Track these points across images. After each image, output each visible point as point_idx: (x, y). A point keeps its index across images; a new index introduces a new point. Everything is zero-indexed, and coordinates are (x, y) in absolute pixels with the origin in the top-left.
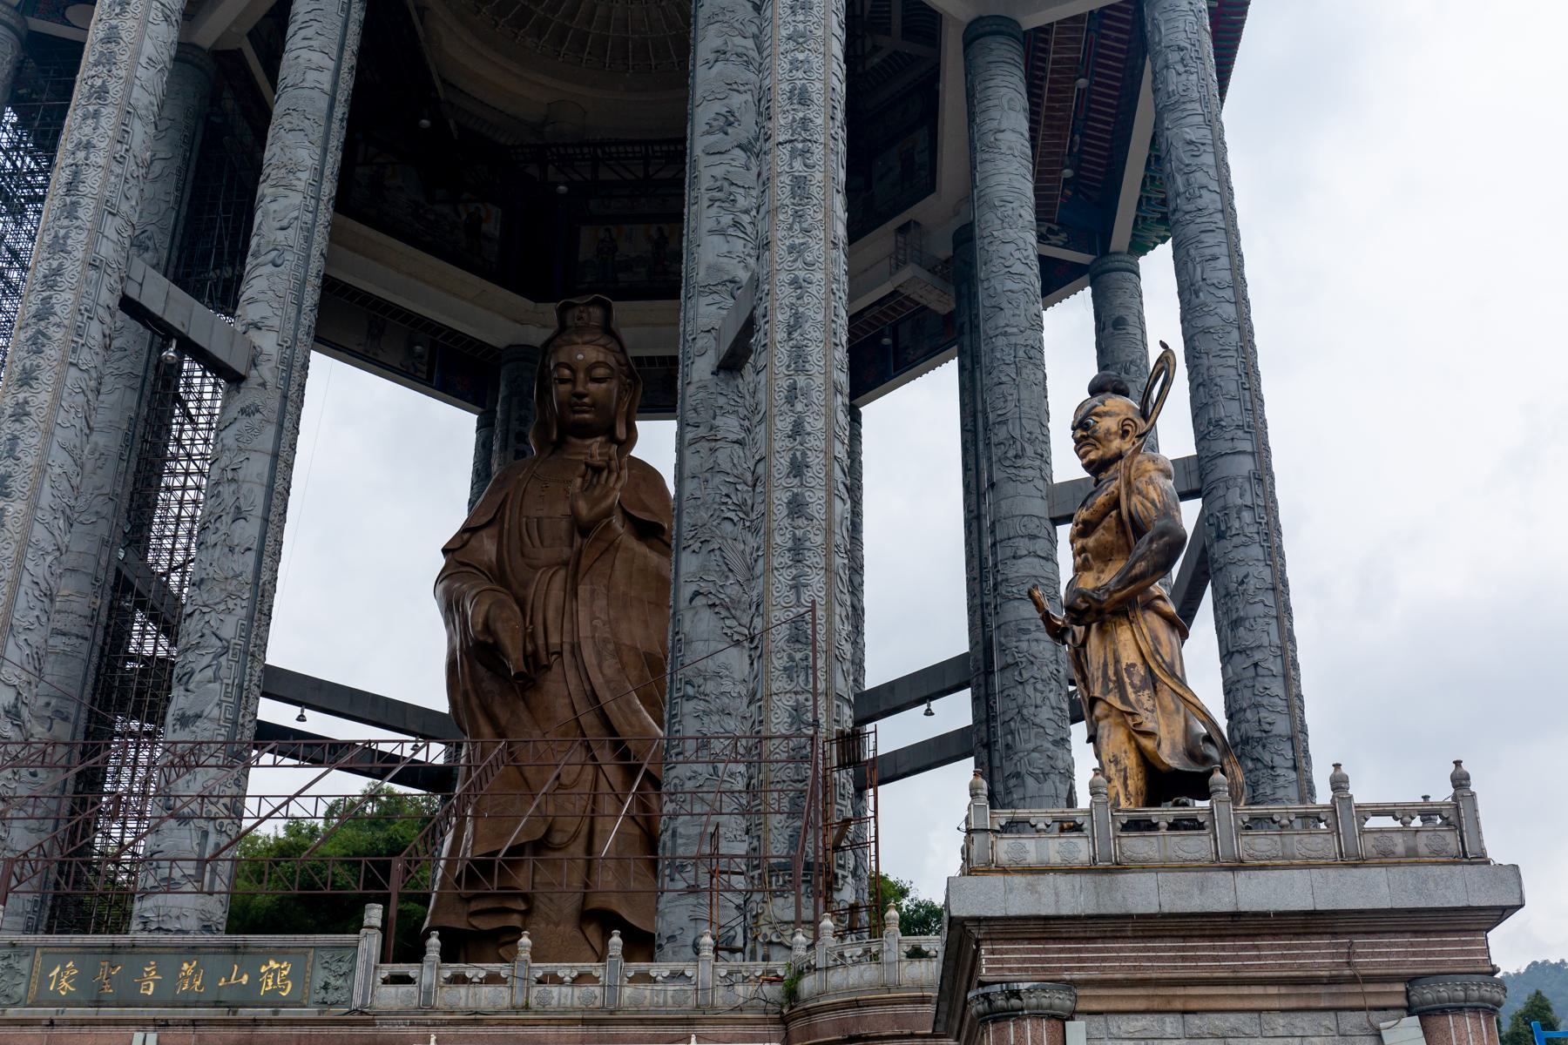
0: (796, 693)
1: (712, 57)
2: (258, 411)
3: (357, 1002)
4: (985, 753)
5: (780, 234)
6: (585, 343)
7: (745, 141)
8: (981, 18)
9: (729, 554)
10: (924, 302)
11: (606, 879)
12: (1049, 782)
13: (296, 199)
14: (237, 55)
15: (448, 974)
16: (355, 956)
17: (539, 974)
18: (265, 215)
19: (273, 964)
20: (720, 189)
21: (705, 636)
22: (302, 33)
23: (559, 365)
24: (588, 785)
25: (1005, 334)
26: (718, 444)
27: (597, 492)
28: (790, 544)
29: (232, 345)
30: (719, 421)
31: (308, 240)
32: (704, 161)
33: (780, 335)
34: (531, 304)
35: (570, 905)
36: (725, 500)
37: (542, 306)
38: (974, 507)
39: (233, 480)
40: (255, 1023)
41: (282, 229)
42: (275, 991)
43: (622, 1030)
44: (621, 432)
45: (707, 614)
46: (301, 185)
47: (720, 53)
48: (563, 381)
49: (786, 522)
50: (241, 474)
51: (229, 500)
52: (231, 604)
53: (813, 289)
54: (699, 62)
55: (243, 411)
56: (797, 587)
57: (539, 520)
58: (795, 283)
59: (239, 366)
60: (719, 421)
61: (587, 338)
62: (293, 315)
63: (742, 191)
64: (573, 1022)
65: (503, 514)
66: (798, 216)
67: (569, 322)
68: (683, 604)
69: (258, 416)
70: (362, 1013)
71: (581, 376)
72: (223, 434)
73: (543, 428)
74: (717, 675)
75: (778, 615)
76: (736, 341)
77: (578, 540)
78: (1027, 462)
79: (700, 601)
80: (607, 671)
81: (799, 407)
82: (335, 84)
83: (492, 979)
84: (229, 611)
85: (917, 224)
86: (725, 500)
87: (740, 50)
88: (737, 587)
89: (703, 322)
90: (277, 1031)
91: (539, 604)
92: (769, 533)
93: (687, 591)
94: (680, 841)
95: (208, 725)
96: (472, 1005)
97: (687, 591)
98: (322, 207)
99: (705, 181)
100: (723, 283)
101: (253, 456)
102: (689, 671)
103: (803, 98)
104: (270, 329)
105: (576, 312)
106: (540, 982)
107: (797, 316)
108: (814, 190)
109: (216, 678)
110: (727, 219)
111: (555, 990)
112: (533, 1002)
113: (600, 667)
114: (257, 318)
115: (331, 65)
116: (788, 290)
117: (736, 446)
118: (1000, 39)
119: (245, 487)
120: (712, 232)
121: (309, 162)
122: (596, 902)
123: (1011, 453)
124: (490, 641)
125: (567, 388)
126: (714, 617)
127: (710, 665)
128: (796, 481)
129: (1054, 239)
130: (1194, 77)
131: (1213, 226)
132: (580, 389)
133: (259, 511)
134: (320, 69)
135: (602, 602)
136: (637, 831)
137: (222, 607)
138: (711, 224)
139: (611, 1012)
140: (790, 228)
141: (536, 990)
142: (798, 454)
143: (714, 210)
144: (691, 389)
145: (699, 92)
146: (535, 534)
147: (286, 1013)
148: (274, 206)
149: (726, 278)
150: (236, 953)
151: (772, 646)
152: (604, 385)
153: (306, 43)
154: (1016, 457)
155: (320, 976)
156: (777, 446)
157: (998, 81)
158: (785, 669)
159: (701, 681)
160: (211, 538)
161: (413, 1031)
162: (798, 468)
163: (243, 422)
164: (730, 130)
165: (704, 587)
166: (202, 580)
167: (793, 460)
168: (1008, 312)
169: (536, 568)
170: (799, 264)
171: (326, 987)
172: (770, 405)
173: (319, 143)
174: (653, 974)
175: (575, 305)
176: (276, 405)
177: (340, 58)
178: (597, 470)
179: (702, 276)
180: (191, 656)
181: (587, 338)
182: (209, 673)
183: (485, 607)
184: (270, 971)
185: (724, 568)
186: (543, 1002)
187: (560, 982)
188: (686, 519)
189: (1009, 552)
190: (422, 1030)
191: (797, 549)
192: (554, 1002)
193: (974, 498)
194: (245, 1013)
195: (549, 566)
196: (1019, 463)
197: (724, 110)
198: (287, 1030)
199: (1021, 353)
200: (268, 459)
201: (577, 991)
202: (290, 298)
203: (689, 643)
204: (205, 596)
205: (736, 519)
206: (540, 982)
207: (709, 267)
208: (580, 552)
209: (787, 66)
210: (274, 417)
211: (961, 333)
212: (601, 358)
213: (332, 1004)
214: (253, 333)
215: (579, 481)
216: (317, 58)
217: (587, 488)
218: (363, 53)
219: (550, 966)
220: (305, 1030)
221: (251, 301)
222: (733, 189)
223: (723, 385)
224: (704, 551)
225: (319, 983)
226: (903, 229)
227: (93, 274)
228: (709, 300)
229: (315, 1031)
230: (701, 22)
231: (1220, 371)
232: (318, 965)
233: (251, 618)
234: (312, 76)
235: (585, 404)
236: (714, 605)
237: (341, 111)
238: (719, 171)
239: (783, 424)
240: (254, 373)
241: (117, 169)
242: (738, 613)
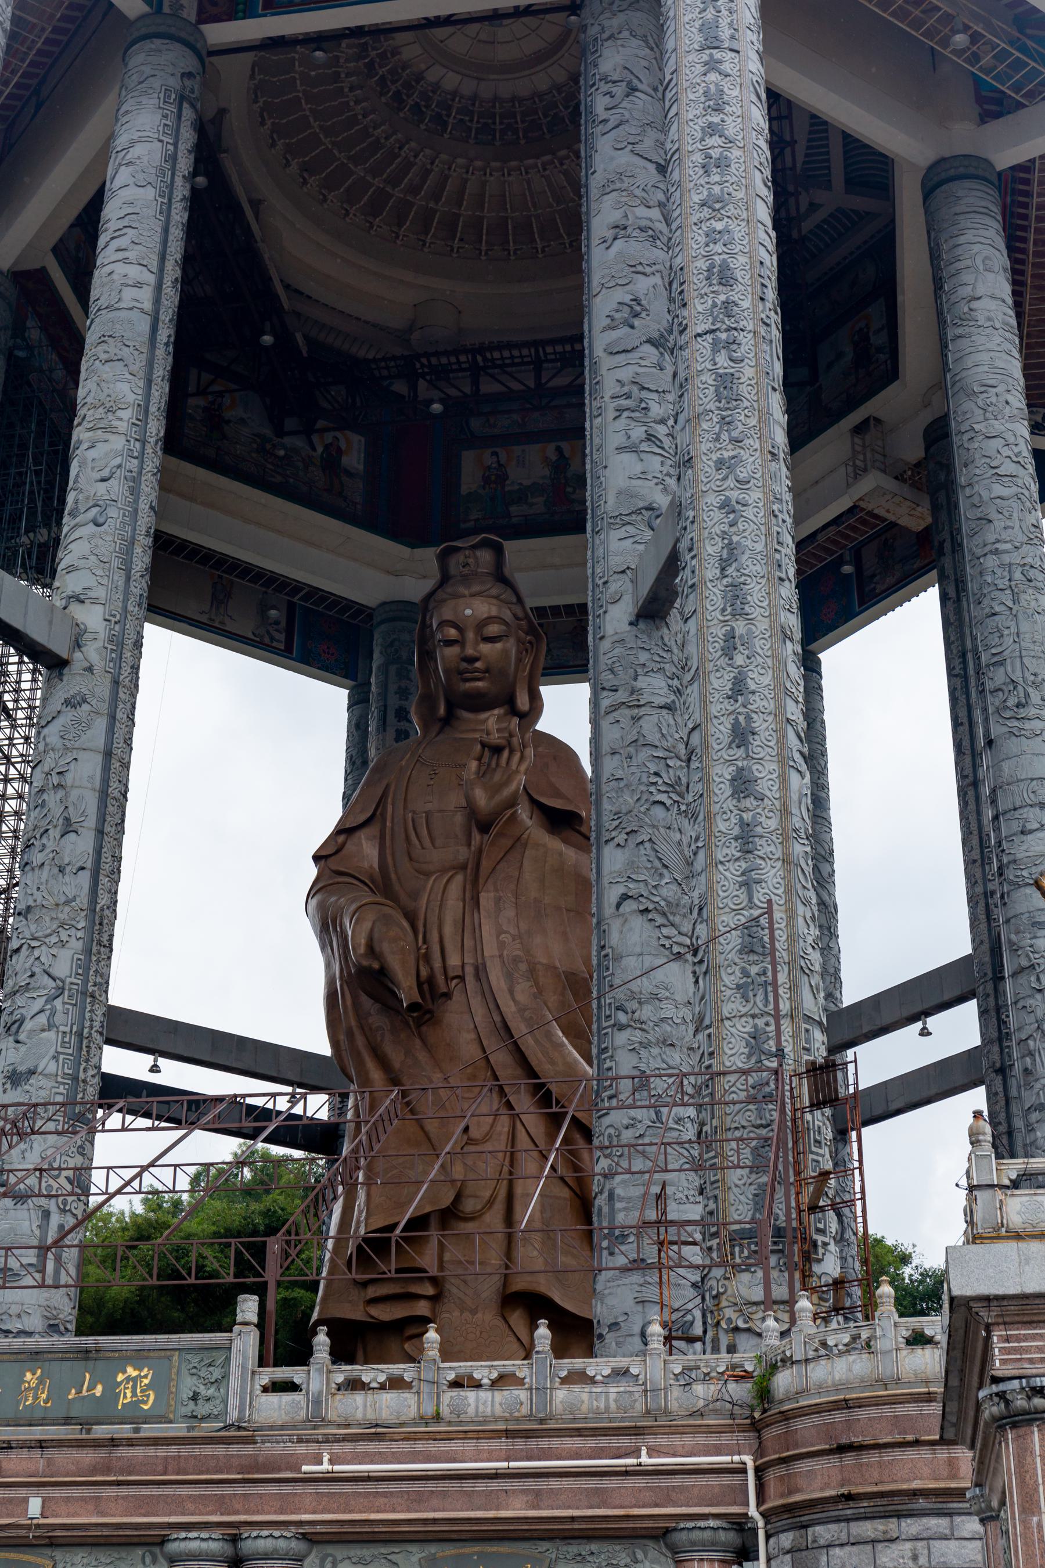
0: (753, 1016)
1: (610, 234)
2: (85, 701)
3: (233, 1415)
4: (998, 1080)
5: (704, 448)
6: (473, 595)
7: (656, 335)
8: (943, 160)
9: (662, 847)
10: (891, 517)
11: (530, 1256)
13: (118, 443)
14: (41, 275)
15: (340, 1378)
16: (228, 1359)
17: (451, 1376)
18: (82, 464)
19: (131, 1371)
20: (628, 396)
21: (638, 950)
22: (114, 244)
23: (442, 624)
24: (504, 1137)
25: (996, 552)
26: (642, 711)
27: (497, 777)
28: (736, 831)
29: (51, 623)
30: (642, 682)
31: (135, 492)
32: (606, 362)
33: (711, 572)
34: (404, 551)
35: (489, 1288)
36: (653, 779)
37: (419, 552)
38: (968, 771)
39: (60, 786)
40: (113, 1442)
41: (103, 480)
42: (135, 1404)
43: (556, 1443)
44: (523, 702)
45: (638, 923)
46: (122, 426)
47: (619, 229)
48: (449, 643)
49: (731, 804)
50: (69, 778)
51: (57, 811)
52: (64, 938)
53: (749, 513)
54: (595, 241)
55: (67, 702)
56: (748, 884)
57: (428, 814)
58: (726, 506)
59: (61, 649)
60: (642, 682)
61: (476, 588)
62: (121, 583)
63: (655, 396)
64: (495, 1434)
65: (385, 809)
66: (726, 422)
67: (453, 570)
68: (609, 910)
69: (85, 707)
70: (239, 1428)
71: (470, 635)
72: (45, 731)
73: (428, 701)
74: (655, 997)
75: (726, 919)
76: (658, 580)
77: (476, 837)
78: (1033, 712)
79: (629, 906)
80: (520, 997)
81: (739, 660)
82: (157, 302)
83: (395, 1383)
84: (63, 944)
85: (878, 421)
86: (653, 779)
87: (644, 223)
88: (674, 887)
89: (616, 562)
90: (139, 1452)
91: (433, 919)
92: (710, 818)
93: (612, 895)
94: (618, 1205)
95: (44, 1082)
96: (371, 1416)
97: (612, 895)
98: (149, 450)
99: (609, 387)
100: (638, 512)
101: (82, 755)
102: (620, 994)
103: (724, 277)
104: (95, 601)
105: (460, 557)
106: (456, 1384)
107: (731, 547)
108: (744, 390)
109: (50, 1026)
111: (471, 1395)
112: (445, 1411)
113: (511, 992)
114: (78, 590)
115: (151, 279)
116: (717, 515)
117: (664, 712)
118: (968, 184)
119: (74, 794)
120: (620, 449)
121: (131, 398)
122: (519, 1284)
123: (1012, 702)
124: (376, 966)
125: (453, 651)
126: (648, 926)
127: (645, 985)
128: (741, 752)
132: (470, 651)
133: (91, 822)
134: (138, 285)
135: (510, 913)
136: (566, 1193)
137: (54, 939)
138: (618, 440)
139: (542, 1421)
140: (717, 439)
141: (449, 1396)
142: (741, 718)
143: (623, 421)
144: (605, 645)
145: (596, 279)
146: (424, 832)
147: (149, 1430)
148: (92, 454)
149: (641, 504)
150: (87, 1359)
151: (720, 959)
152: (499, 646)
153: (121, 255)
154: (1019, 705)
155: (188, 1385)
156: (714, 710)
157: (969, 236)
158: (739, 987)
159: (634, 1005)
160: (37, 858)
161: (302, 1449)
162: (741, 736)
163: (68, 716)
164: (636, 322)
165: (634, 889)
166: (29, 908)
167: (736, 726)
168: (999, 524)
169: (428, 874)
170: (730, 482)
171: (195, 1397)
172: (703, 659)
173: (142, 374)
174: (590, 1372)
175: (457, 549)
176: (105, 692)
177: (161, 269)
178: (497, 750)
179: (611, 504)
180: (20, 1001)
181: (476, 588)
182: (42, 1019)
183: (367, 925)
184: (128, 1379)
185: (657, 864)
186: (458, 1410)
187: (478, 1386)
188: (607, 806)
189: (1016, 827)
190: (313, 1448)
191: (746, 838)
192: (471, 1411)
193: (968, 759)
194: (101, 1431)
195: (443, 871)
196: (1023, 712)
197: (627, 298)
198: (151, 1451)
199: (1018, 575)
200: (99, 758)
201: (500, 1396)
202: (116, 563)
203: (618, 958)
204: (33, 927)
205: (668, 802)
206: (456, 1384)
207: (620, 493)
208: (480, 851)
209: (702, 239)
210: (104, 708)
211: (941, 553)
212: (494, 612)
213: (204, 1419)
214: (75, 609)
215: (474, 765)
216: (134, 272)
217: (483, 773)
218: (188, 261)
219: (463, 1367)
220: (173, 1451)
221: (71, 569)
222: (644, 394)
223: (645, 638)
224: (631, 843)
225: (186, 1394)
226: (860, 429)
228: (622, 533)
229: (185, 1451)
230: (594, 193)
232: (185, 1372)
233: (88, 952)
234: (129, 293)
235: (477, 670)
236: (647, 910)
237: (166, 333)
238: (626, 374)
239: (721, 682)
240: (77, 655)
242: (677, 920)
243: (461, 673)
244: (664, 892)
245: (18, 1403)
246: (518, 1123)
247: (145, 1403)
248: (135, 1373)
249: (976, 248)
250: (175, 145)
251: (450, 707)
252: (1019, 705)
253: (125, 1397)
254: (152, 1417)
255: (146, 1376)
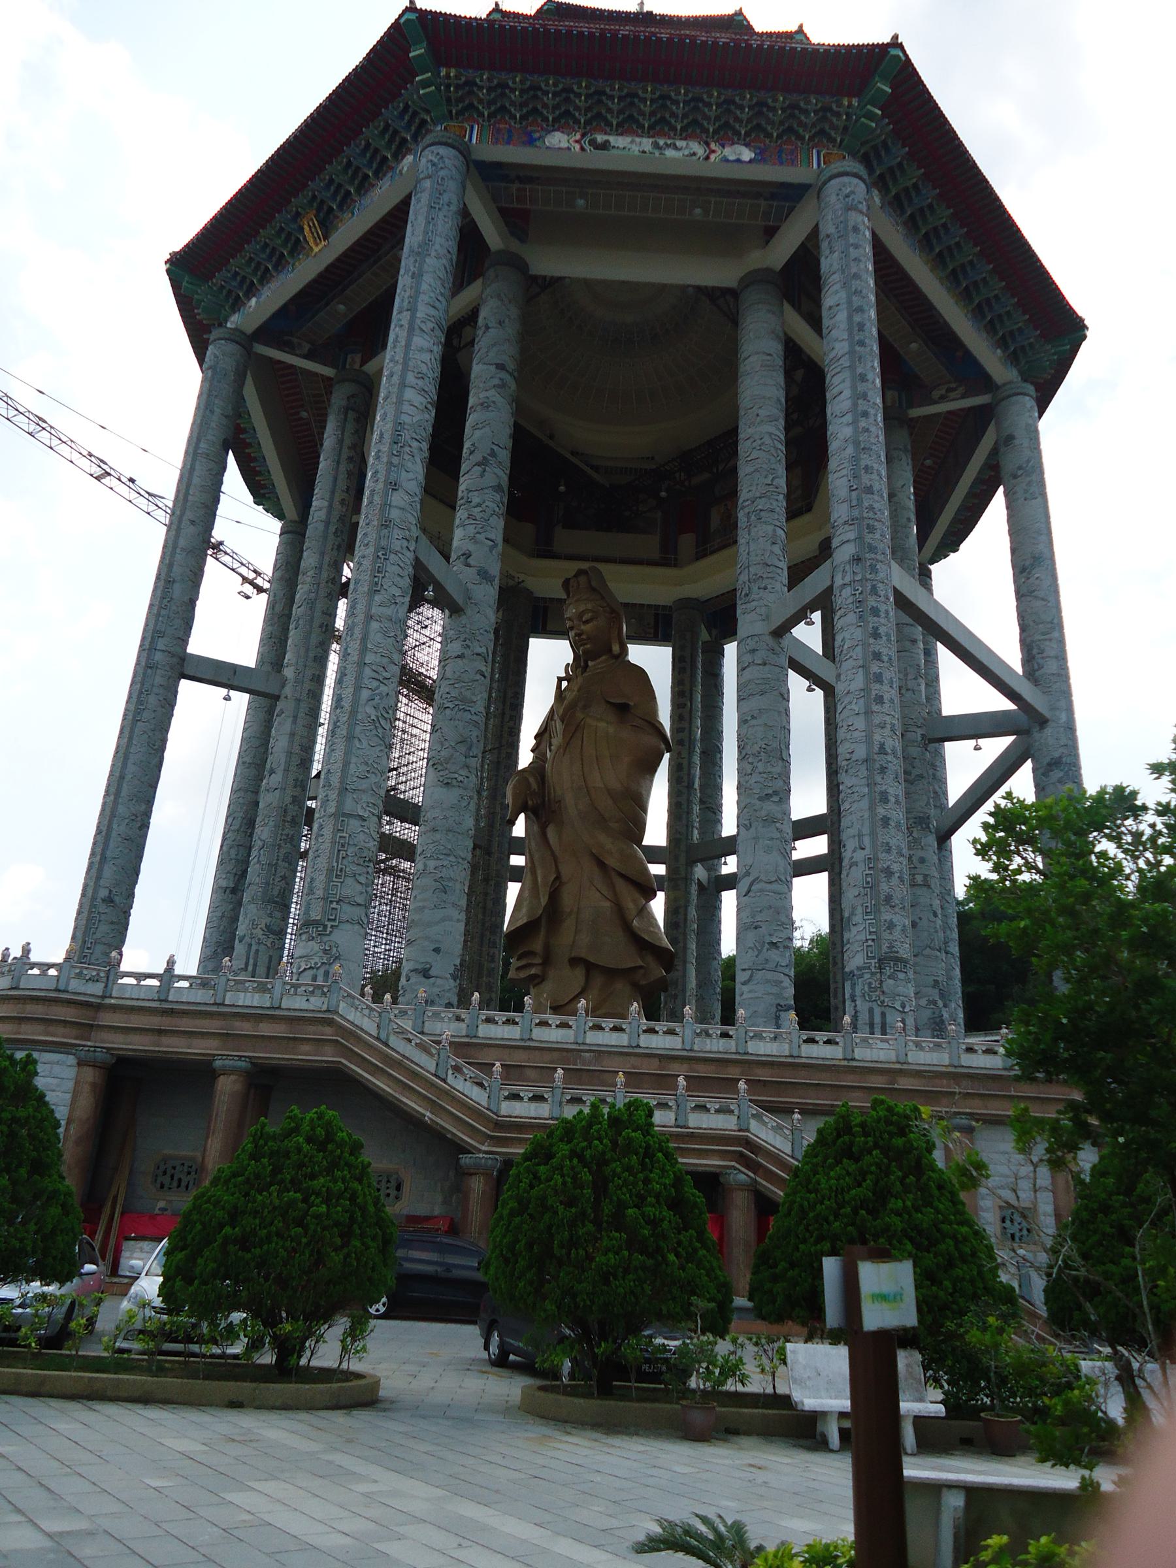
12: (752, 830)
44: (616, 649)
82: (329, 513)
104: (291, 665)
110: (466, 515)
115: (326, 504)
129: (952, 395)
130: (836, 254)
131: (838, 369)
133: (282, 767)
136: (607, 904)
154: (747, 595)
227: (149, 671)
231: (838, 483)
241: (163, 612)
242: (448, 766)
244: (442, 753)
249: (751, 327)
250: (343, 434)
252: (747, 595)
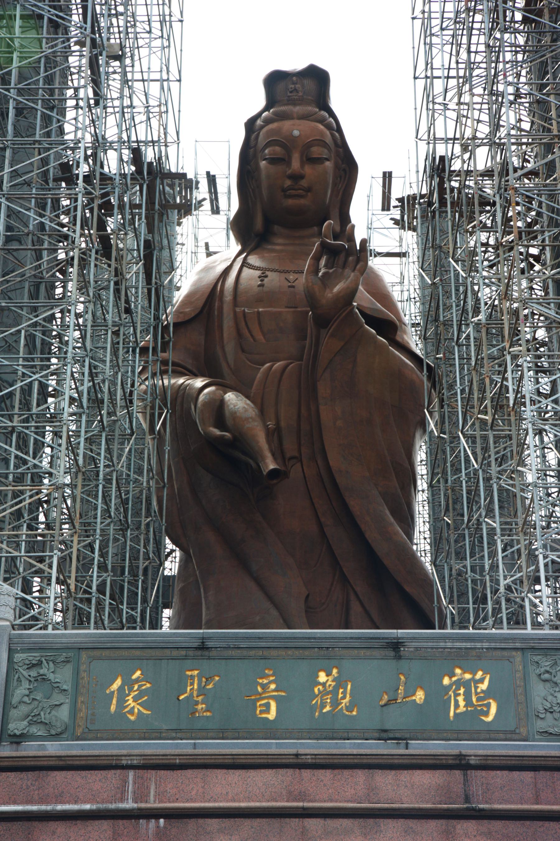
184: (459, 683)
232: (533, 678)
243: (284, 190)
245: (313, 709)
246: (352, 597)
247: (487, 714)
248: (468, 676)
251: (268, 222)
253: (457, 706)
254: (498, 732)
255: (482, 681)
